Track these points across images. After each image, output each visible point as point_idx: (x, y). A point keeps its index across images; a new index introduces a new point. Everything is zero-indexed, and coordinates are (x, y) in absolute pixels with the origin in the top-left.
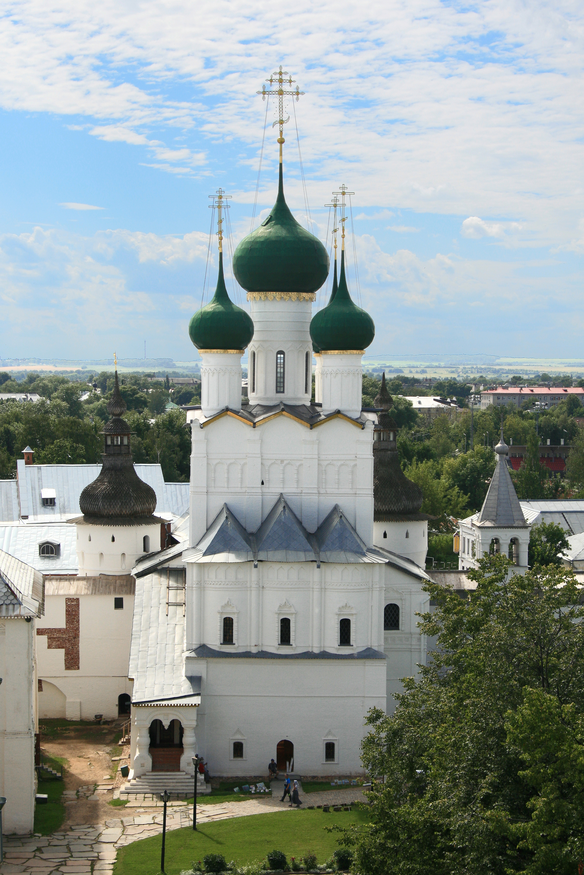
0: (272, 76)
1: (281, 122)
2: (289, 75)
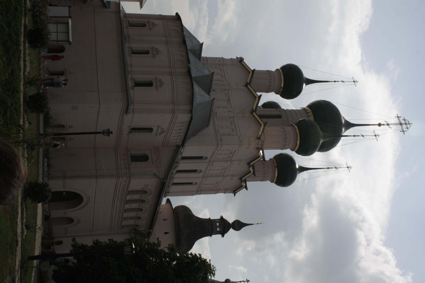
0: (406, 120)
1: (388, 125)
2: (410, 127)
